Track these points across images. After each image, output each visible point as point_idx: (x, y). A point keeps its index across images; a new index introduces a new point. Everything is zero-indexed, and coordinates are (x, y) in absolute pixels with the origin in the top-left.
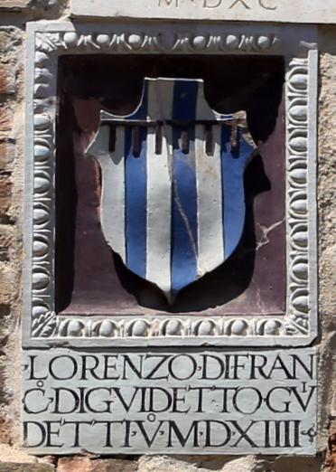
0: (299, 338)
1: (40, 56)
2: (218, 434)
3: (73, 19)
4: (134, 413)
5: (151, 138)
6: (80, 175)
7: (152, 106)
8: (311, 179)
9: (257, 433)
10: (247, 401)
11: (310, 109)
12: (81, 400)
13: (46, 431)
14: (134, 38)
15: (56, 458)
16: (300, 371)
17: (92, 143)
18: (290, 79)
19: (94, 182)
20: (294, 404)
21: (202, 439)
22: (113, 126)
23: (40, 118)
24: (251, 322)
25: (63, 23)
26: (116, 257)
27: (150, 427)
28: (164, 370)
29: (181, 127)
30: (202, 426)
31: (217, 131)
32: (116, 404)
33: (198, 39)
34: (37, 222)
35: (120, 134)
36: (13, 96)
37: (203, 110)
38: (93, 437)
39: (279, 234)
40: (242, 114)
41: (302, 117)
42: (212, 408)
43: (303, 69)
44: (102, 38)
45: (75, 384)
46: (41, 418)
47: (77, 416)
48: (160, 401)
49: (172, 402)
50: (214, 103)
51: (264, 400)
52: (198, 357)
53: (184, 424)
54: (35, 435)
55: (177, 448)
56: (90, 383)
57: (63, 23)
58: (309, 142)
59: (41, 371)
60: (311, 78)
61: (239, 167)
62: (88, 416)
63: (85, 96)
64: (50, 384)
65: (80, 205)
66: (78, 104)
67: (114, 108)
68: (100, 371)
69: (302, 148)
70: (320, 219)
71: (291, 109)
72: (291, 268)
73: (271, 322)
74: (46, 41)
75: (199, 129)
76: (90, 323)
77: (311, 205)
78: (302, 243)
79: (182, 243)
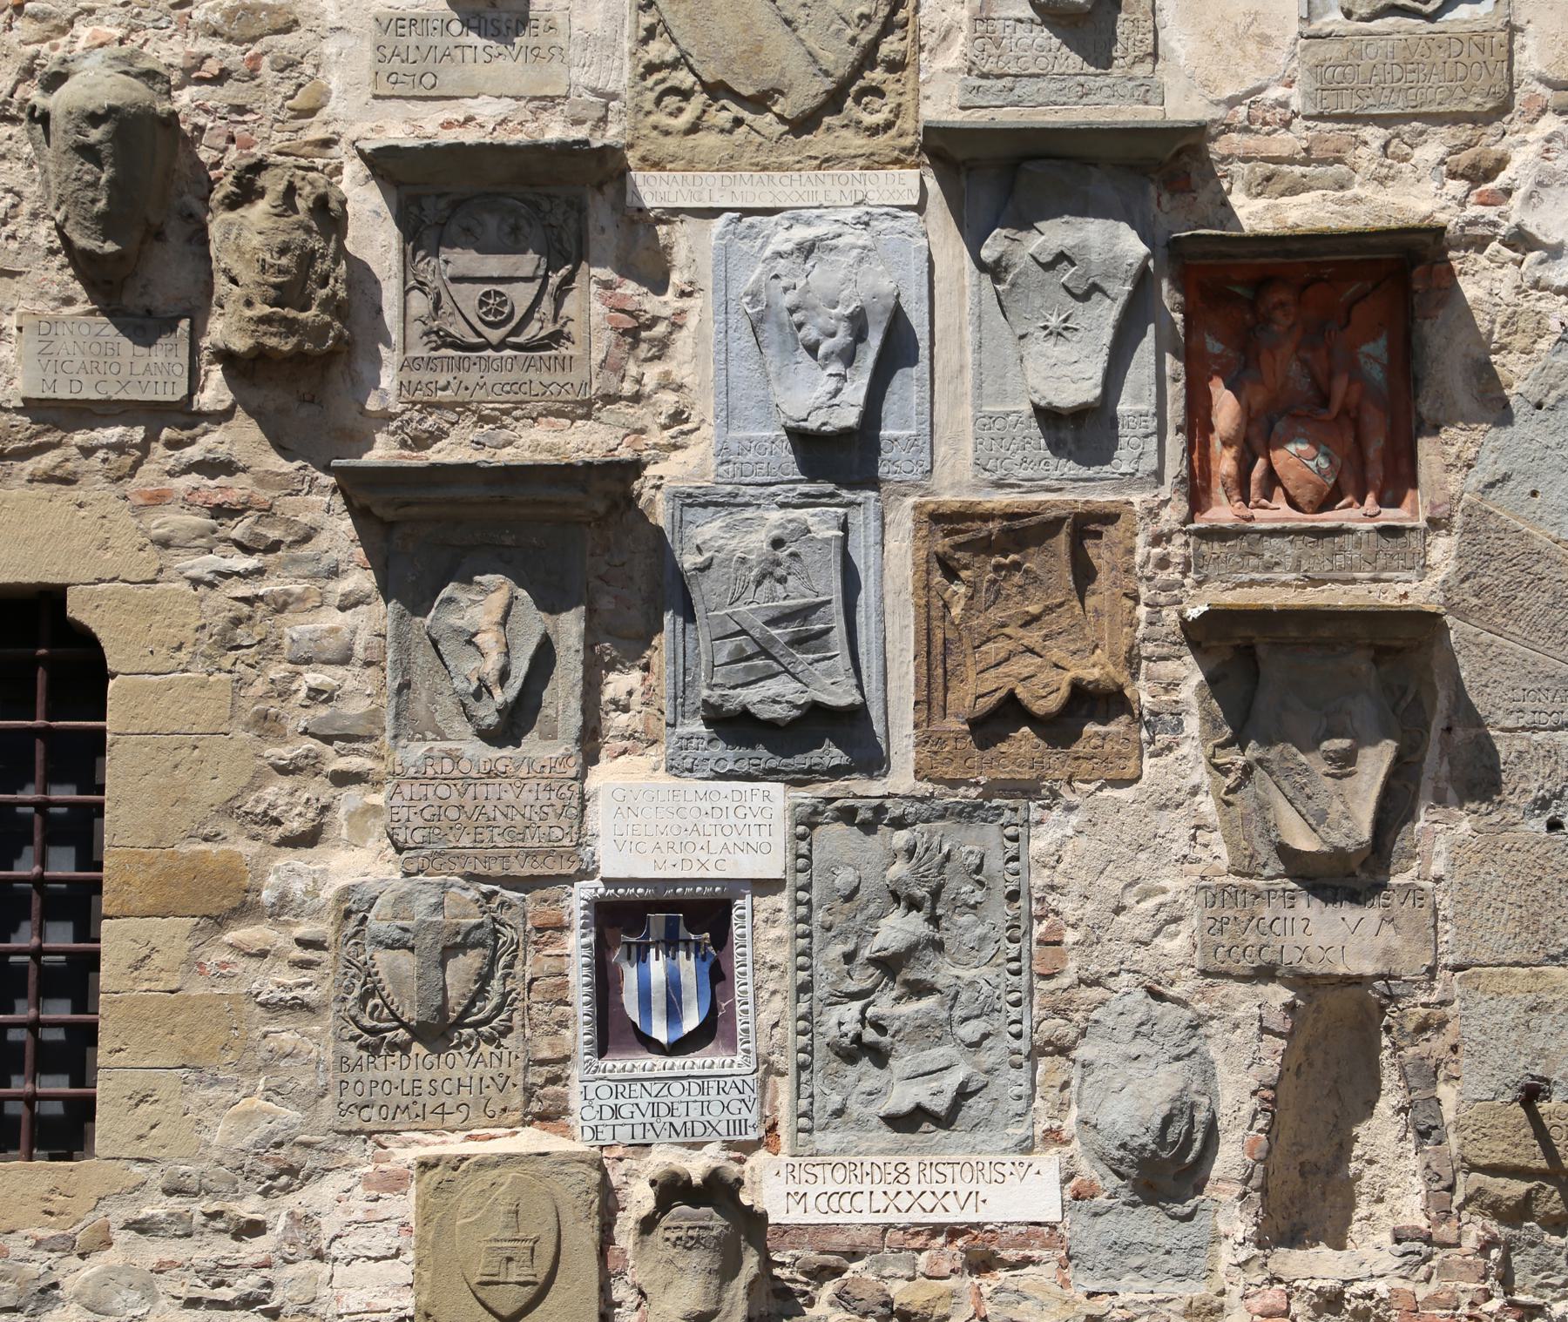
0: (745, 1069)
1: (583, 903)
2: (699, 1129)
3: (602, 879)
4: (648, 1118)
5: (653, 951)
6: (610, 975)
7: (653, 931)
8: (750, 973)
9: (722, 1128)
10: (716, 1108)
11: (748, 931)
12: (616, 1111)
13: (595, 1131)
14: (640, 891)
15: (602, 1147)
16: (747, 1089)
17: (617, 955)
18: (735, 913)
19: (619, 978)
20: (744, 1109)
21: (689, 1133)
22: (629, 944)
23: (585, 941)
24: (717, 1060)
25: (597, 882)
26: (634, 1024)
27: (658, 1127)
28: (665, 1091)
29: (671, 944)
30: (689, 1125)
31: (692, 946)
32: (637, 1112)
33: (679, 890)
34: (585, 1004)
35: (634, 949)
36: (568, 928)
37: (683, 933)
38: (624, 1134)
39: (732, 1007)
40: (707, 935)
41: (743, 936)
42: (695, 1113)
43: (743, 906)
44: (621, 891)
45: (612, 1101)
46: (592, 1124)
47: (613, 1121)
48: (663, 1110)
49: (671, 1111)
50: (690, 929)
51: (726, 1107)
52: (685, 1083)
53: (678, 1126)
54: (588, 1133)
55: (675, 1139)
56: (621, 1101)
57: (597, 882)
58: (748, 950)
59: (591, 1095)
60: (747, 912)
61: (706, 967)
62: (620, 1121)
63: (612, 926)
64: (597, 1103)
65: (611, 993)
66: (608, 932)
67: (629, 933)
68: (626, 1094)
69: (743, 955)
70: (756, 997)
71: (736, 931)
72: (739, 1027)
73: (728, 1061)
74: (587, 894)
75: (681, 945)
76: (619, 1065)
77: (750, 988)
78: (746, 1012)
79: (674, 1014)
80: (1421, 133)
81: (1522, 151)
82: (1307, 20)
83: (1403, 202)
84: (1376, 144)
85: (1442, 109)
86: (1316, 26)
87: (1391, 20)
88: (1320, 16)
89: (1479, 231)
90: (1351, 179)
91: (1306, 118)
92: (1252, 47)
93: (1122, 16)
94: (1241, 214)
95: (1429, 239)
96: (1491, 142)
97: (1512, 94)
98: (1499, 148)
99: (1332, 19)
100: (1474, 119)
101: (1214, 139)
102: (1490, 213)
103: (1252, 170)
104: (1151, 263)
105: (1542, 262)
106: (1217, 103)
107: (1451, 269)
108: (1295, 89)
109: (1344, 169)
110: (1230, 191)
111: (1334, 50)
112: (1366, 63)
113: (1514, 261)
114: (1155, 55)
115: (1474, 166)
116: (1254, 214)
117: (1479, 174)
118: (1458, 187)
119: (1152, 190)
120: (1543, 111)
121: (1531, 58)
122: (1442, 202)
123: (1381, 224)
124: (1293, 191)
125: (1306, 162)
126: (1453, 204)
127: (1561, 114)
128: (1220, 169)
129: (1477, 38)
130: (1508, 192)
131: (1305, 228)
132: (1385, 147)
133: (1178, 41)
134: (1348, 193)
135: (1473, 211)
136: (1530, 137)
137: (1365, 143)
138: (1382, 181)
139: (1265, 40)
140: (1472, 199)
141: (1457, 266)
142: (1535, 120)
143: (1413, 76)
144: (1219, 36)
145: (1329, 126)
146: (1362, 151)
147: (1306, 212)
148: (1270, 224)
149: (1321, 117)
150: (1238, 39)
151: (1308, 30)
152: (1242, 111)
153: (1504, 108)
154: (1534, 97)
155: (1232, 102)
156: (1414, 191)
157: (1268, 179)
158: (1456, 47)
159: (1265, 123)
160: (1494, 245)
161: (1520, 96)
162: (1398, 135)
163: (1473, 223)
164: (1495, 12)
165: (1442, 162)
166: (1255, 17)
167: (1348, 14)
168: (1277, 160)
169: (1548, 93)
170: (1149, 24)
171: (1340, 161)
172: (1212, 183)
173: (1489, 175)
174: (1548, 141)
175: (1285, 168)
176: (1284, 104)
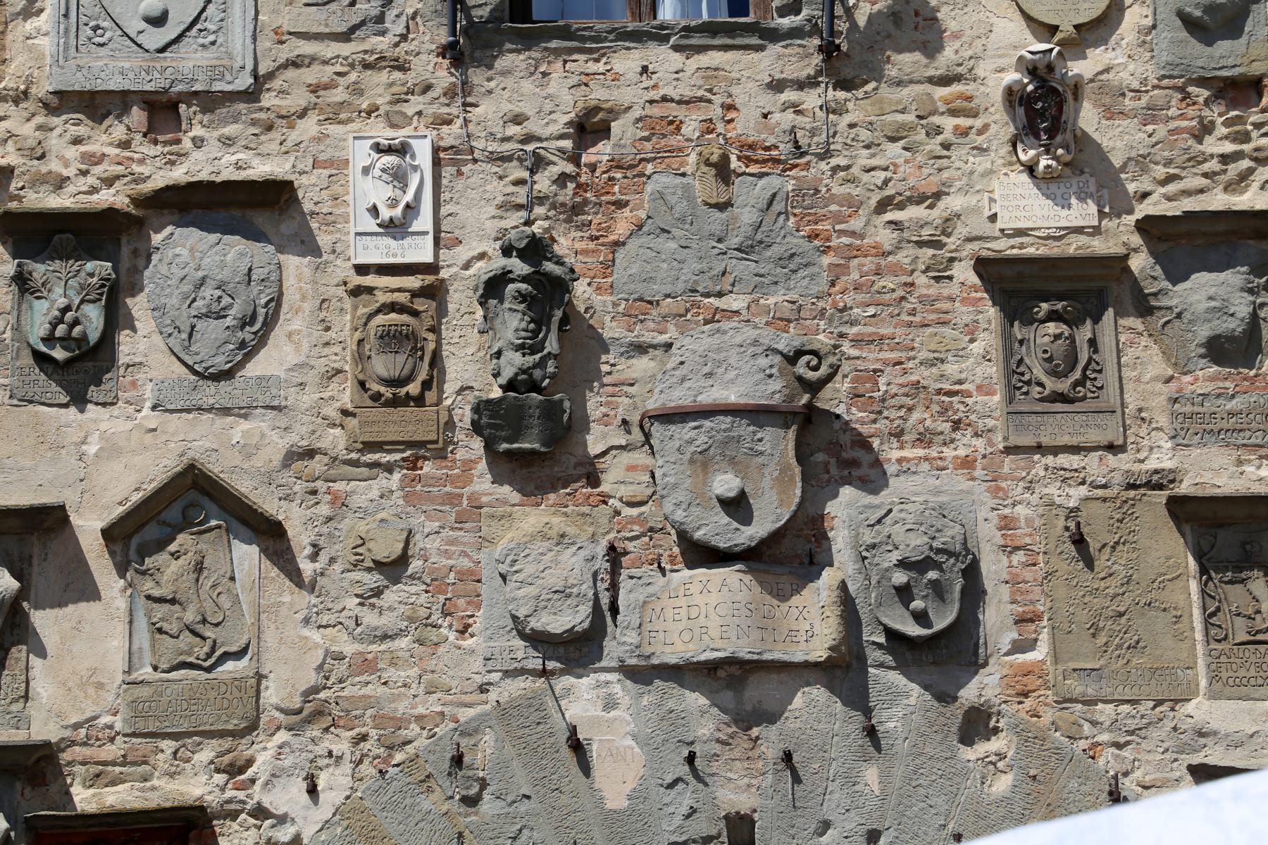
80: (199, 744)
81: (263, 755)
82: (129, 672)
83: (184, 789)
84: (169, 752)
85: (212, 728)
86: (135, 676)
87: (183, 672)
88: (137, 670)
89: (233, 807)
90: (152, 774)
91: (125, 735)
92: (91, 691)
93: (6, 672)
94: (76, 799)
95: (197, 813)
96: (244, 749)
97: (258, 718)
98: (249, 752)
99: (146, 672)
100: (233, 734)
101: (63, 751)
102: (241, 795)
103: (87, 771)
104: (12, 834)
105: (273, 826)
106: (66, 727)
107: (214, 832)
108: (119, 717)
109: (147, 768)
110: (71, 785)
111: (144, 692)
112: (165, 699)
113: (255, 826)
114: (26, 697)
115: (231, 765)
116: (85, 799)
117: (235, 770)
118: (220, 778)
119: (18, 786)
120: (279, 728)
121: (272, 695)
122: (209, 789)
123: (168, 804)
124: (113, 783)
125: (123, 764)
126: (216, 789)
127: (290, 730)
128: (66, 770)
129: (238, 681)
130: (253, 781)
131: (119, 807)
132: (175, 753)
133: (43, 687)
134: (148, 784)
135: (229, 794)
136: (269, 745)
137: (162, 751)
138: (172, 775)
139: (100, 686)
140: (230, 786)
141: (217, 830)
142: (273, 735)
143: (195, 707)
144: (70, 684)
145: (139, 740)
146: (160, 756)
147: (121, 797)
148: (94, 806)
149: (134, 735)
150: (82, 686)
151: (129, 679)
152: (83, 732)
153: (253, 727)
154: (273, 719)
155: (77, 726)
156: (192, 781)
157: (98, 776)
158: (223, 689)
159: (98, 739)
160: (243, 816)
161: (264, 719)
162: (184, 746)
163: (229, 801)
164: (249, 666)
165: (212, 762)
166: (94, 671)
167: (155, 668)
168: (105, 763)
169: (281, 717)
170: (23, 677)
171: (145, 763)
172: (61, 779)
173: (242, 770)
174: (280, 747)
175: (110, 768)
176: (111, 727)
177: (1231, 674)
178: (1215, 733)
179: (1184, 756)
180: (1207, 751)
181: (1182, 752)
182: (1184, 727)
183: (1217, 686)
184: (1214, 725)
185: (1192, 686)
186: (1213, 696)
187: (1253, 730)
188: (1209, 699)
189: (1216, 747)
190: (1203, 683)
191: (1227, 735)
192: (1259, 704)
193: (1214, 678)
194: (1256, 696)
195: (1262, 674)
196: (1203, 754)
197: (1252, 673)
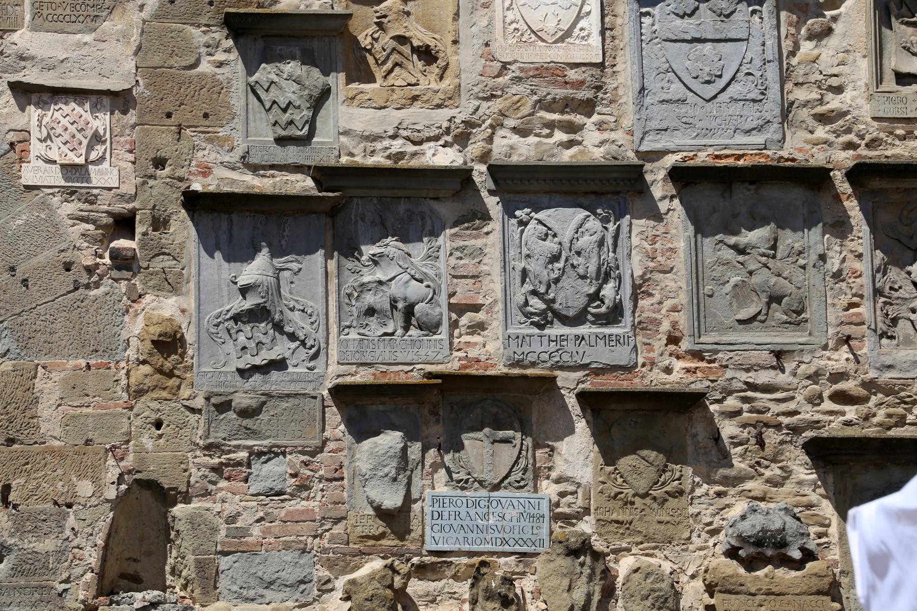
177: (50, 11)
178: (33, 58)
179: (6, 75)
180: (26, 72)
181: (6, 72)
182: (9, 52)
183: (38, 21)
184: (32, 52)
185: (19, 20)
186: (34, 28)
187: (64, 56)
188: (31, 31)
189: (33, 69)
190: (28, 17)
191: (43, 60)
192: (71, 36)
193: (36, 14)
194: (69, 30)
195: (75, 13)
196: (22, 74)
197: (68, 11)
